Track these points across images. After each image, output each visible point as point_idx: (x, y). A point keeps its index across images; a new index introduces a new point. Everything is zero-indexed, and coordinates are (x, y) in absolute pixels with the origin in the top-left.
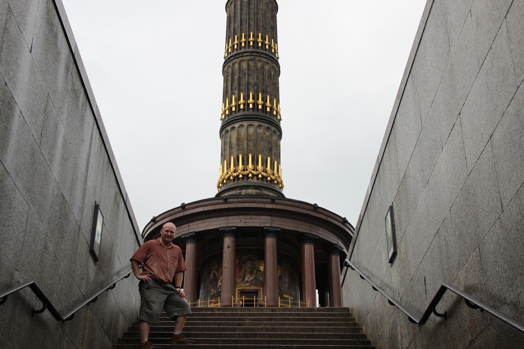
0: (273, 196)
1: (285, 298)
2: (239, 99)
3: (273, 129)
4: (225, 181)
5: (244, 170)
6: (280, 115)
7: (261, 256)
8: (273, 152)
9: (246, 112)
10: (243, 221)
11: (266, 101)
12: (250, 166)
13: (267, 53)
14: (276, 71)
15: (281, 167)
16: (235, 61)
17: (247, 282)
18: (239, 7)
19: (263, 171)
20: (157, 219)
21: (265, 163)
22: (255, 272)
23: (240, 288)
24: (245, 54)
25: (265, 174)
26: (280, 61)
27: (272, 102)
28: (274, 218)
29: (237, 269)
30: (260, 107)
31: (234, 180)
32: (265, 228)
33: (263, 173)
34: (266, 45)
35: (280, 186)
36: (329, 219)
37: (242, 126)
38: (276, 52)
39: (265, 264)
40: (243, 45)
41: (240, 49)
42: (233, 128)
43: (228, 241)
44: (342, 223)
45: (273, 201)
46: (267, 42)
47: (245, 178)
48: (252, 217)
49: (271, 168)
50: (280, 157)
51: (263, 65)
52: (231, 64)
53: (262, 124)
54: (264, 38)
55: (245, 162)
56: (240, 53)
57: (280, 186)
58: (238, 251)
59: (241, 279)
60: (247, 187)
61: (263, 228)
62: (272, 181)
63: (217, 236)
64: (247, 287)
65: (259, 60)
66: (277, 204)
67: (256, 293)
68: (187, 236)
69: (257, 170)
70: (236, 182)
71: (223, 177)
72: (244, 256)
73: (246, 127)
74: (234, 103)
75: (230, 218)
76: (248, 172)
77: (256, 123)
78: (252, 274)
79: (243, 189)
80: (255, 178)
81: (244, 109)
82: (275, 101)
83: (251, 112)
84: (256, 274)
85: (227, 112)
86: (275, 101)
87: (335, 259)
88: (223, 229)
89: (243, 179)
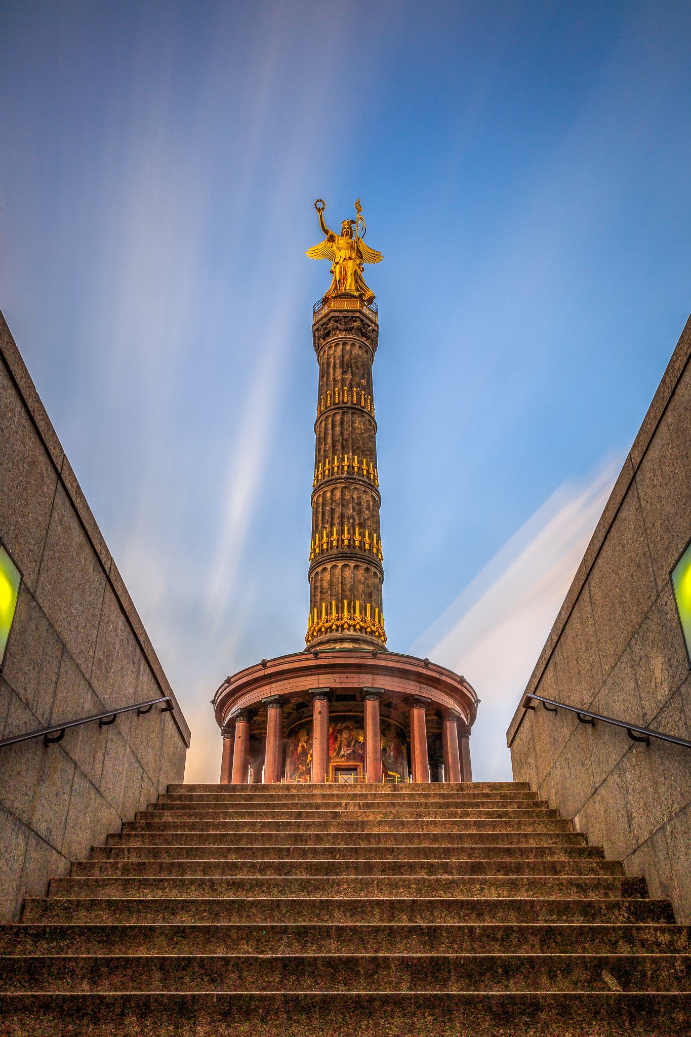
1: (390, 776)
2: (332, 535)
3: (373, 570)
4: (315, 634)
5: (338, 620)
7: (360, 723)
12: (346, 614)
15: (384, 616)
16: (326, 489)
18: (330, 426)
21: (363, 609)
25: (364, 625)
28: (376, 677)
29: (331, 741)
30: (357, 543)
36: (444, 678)
39: (365, 733)
42: (325, 569)
43: (319, 705)
46: (364, 467)
48: (349, 675)
55: (340, 609)
60: (342, 640)
61: (362, 689)
62: (372, 632)
66: (380, 659)
68: (269, 700)
74: (325, 539)
77: (352, 564)
80: (352, 628)
81: (337, 547)
84: (354, 746)
85: (317, 551)
87: (452, 729)
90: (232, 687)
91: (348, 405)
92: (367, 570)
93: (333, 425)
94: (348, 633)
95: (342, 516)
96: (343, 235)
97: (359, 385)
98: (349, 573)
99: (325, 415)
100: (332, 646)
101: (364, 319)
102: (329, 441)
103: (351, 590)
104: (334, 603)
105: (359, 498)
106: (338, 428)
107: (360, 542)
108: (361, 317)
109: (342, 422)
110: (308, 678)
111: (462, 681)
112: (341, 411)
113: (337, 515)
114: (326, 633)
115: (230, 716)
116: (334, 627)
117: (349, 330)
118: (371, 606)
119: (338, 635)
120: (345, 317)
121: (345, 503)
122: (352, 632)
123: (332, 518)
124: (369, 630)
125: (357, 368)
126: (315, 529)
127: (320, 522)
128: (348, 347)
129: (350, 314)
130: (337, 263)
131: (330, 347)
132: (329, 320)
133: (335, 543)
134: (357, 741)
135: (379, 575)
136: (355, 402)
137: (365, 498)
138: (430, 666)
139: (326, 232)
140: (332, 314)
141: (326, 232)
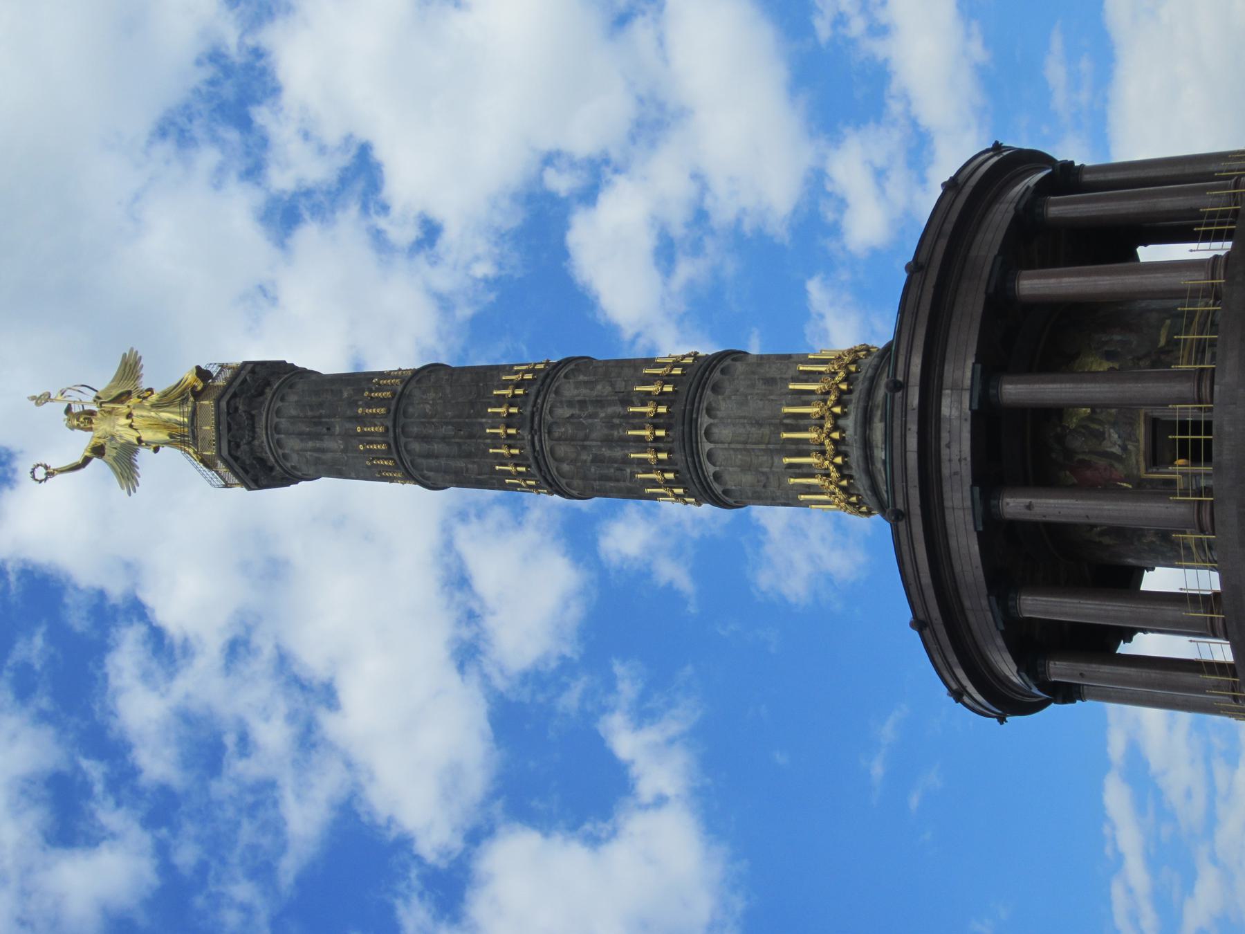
0: (887, 386)
2: (645, 460)
3: (717, 375)
4: (854, 499)
5: (823, 453)
6: (684, 357)
9: (676, 445)
10: (956, 466)
11: (649, 393)
12: (812, 435)
14: (577, 370)
16: (554, 472)
17: (1124, 448)
18: (432, 462)
19: (825, 401)
20: (954, 686)
21: (802, 398)
22: (1096, 427)
24: (538, 448)
30: (662, 410)
31: (850, 477)
32: (975, 407)
34: (514, 396)
35: (861, 354)
36: (948, 227)
37: (710, 456)
40: (515, 451)
43: (1014, 505)
44: (959, 193)
45: (898, 386)
46: (508, 392)
47: (843, 448)
48: (943, 443)
49: (815, 381)
51: (561, 402)
52: (563, 481)
53: (704, 405)
54: (500, 401)
55: (801, 448)
56: (536, 458)
57: (861, 354)
58: (1043, 477)
59: (1117, 465)
60: (867, 445)
61: (975, 414)
63: (998, 535)
64: (1138, 448)
65: (551, 412)
67: (1157, 427)
69: (822, 417)
70: (854, 473)
71: (843, 504)
72: (1054, 456)
73: (712, 446)
75: (948, 504)
76: (827, 441)
77: (705, 421)
78: (1103, 433)
79: (872, 457)
80: (841, 422)
81: (670, 452)
84: (1101, 423)
85: (680, 491)
87: (1060, 208)
88: (980, 523)
89: (845, 455)
90: (971, 689)
91: (390, 424)
92: (716, 389)
93: (429, 455)
94: (850, 433)
95: (608, 441)
96: (91, 429)
97: (353, 404)
98: (725, 425)
99: (411, 470)
100: (879, 465)
101: (231, 391)
102: (461, 464)
103: (759, 424)
104: (787, 460)
105: (570, 404)
106: (437, 447)
107: (659, 404)
108: (227, 397)
109: (425, 438)
110: (951, 531)
112: (403, 440)
113: (606, 452)
114: (850, 477)
115: (1035, 690)
116: (838, 460)
117: (252, 417)
118: (796, 380)
119: (855, 453)
120: (229, 430)
121: (581, 434)
122: (849, 423)
123: (614, 461)
124: (844, 387)
125: (321, 405)
127: (622, 484)
129: (224, 418)
131: (285, 457)
132: (236, 459)
133: (663, 456)
134: (1090, 418)
136: (383, 410)
137: (570, 391)
138: (922, 259)
139: (86, 461)
140: (225, 452)
141: (86, 461)
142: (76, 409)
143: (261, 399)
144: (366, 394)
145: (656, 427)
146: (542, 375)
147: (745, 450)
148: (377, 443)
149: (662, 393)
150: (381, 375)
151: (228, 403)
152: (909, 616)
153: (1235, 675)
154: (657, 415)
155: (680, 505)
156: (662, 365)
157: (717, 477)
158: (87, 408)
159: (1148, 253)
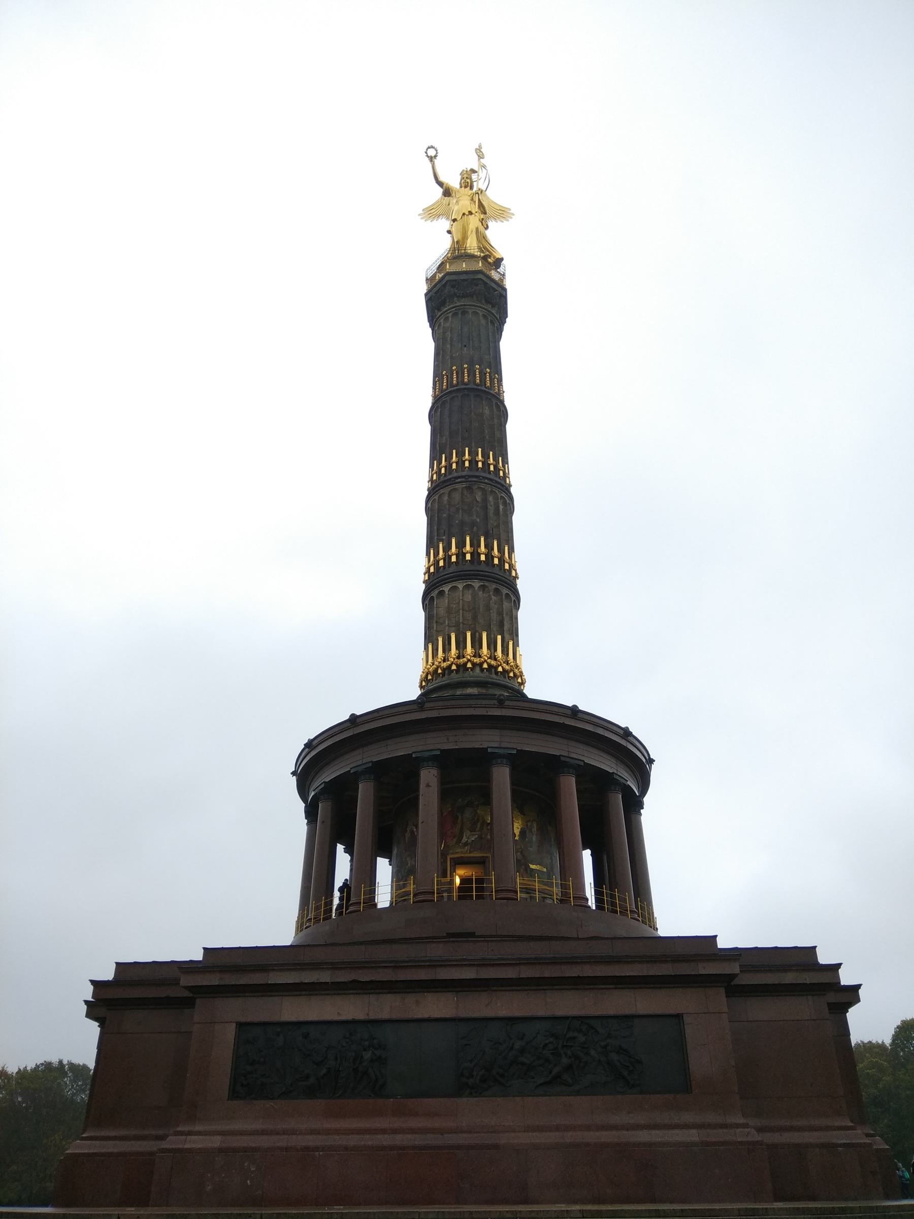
3: (505, 591)
4: (430, 677)
5: (458, 658)
8: (506, 628)
11: (493, 549)
12: (469, 649)
13: (492, 477)
14: (505, 503)
15: (521, 650)
16: (442, 491)
19: (490, 658)
21: (492, 645)
23: (452, 856)
25: (493, 663)
26: (513, 490)
27: (501, 550)
30: (483, 558)
31: (443, 674)
33: (489, 661)
35: (519, 680)
36: (601, 731)
37: (454, 588)
38: (506, 476)
40: (454, 466)
41: (450, 474)
45: (501, 703)
46: (491, 461)
47: (461, 670)
50: (517, 635)
54: (486, 456)
55: (461, 645)
57: (519, 680)
62: (505, 672)
64: (466, 852)
66: (509, 707)
68: (360, 769)
69: (480, 657)
76: (465, 660)
77: (476, 584)
79: (458, 688)
80: (478, 669)
82: (506, 548)
83: (468, 567)
85: (432, 570)
86: (506, 548)
88: (418, 755)
89: (457, 671)
100: (450, 693)
107: (486, 556)
108: (484, 279)
111: (627, 733)
116: (454, 667)
117: (470, 295)
120: (464, 280)
124: (500, 669)
126: (431, 543)
128: (470, 316)
129: (472, 276)
130: (454, 220)
131: (446, 319)
132: (444, 286)
133: (454, 559)
134: (484, 822)
135: (513, 598)
138: (580, 715)
140: (447, 278)
141: (440, 184)
142: (474, 177)
143: (483, 301)
144: (488, 370)
145: (472, 554)
146: (503, 482)
147: (458, 611)
148: (457, 378)
149: (493, 557)
150: (500, 380)
151: (480, 279)
152: (359, 712)
153: (324, 919)
154: (479, 555)
155: (424, 570)
156: (510, 557)
157: (442, 593)
158: (475, 184)
159: (587, 856)
